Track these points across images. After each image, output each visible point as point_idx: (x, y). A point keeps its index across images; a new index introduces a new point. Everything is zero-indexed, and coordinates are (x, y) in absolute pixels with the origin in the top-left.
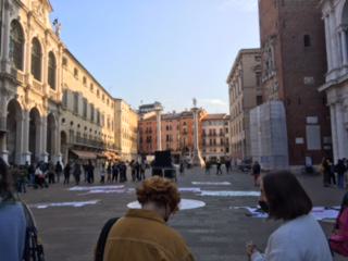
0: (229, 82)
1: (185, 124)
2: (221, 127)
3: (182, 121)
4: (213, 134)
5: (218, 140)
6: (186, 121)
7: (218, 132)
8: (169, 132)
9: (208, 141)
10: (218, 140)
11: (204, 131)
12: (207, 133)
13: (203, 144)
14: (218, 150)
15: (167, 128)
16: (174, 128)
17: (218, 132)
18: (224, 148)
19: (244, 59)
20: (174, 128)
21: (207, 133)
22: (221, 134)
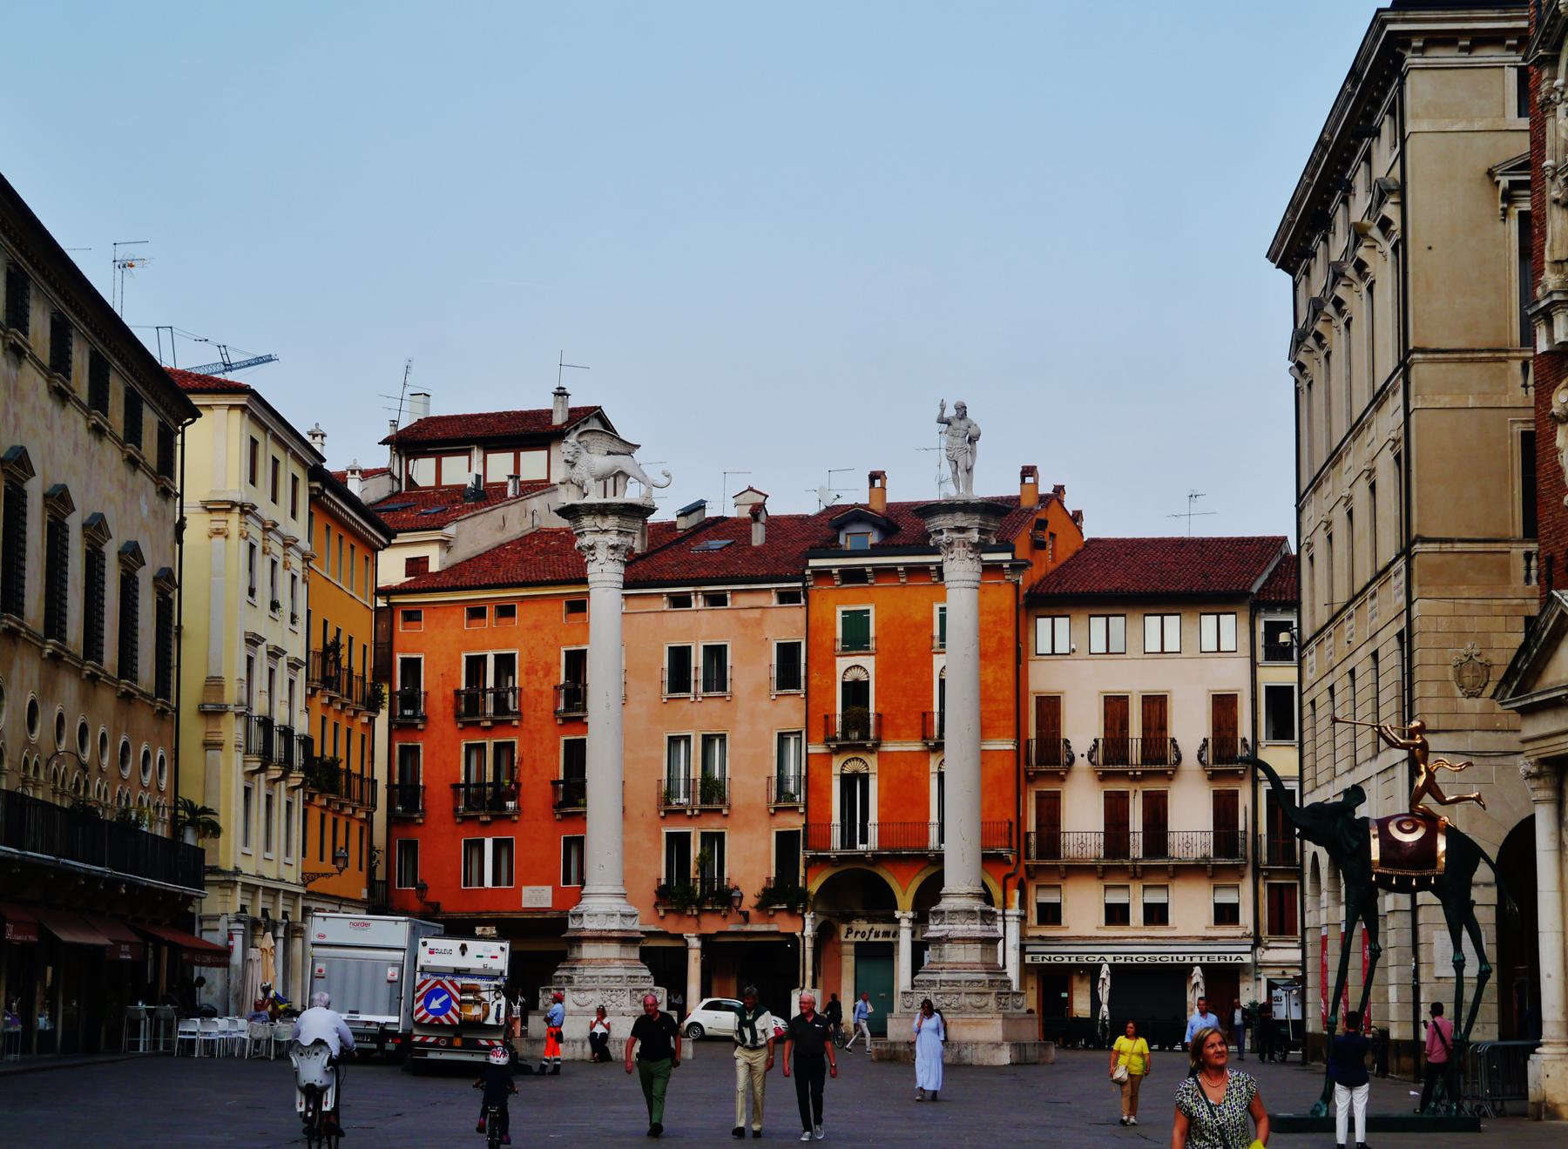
0: (1292, 251)
1: (856, 635)
2: (1233, 676)
3: (836, 608)
4: (1136, 745)
5: (1191, 816)
6: (874, 606)
7: (1190, 728)
8: (697, 714)
9: (1083, 814)
10: (1191, 816)
11: (1050, 707)
12: (1082, 729)
13: (1026, 855)
14: (1191, 909)
15: (717, 677)
16: (752, 670)
17: (1190, 728)
18: (1243, 896)
19: (1424, 89)
20: (752, 670)
21: (1082, 729)
22: (1226, 756)
